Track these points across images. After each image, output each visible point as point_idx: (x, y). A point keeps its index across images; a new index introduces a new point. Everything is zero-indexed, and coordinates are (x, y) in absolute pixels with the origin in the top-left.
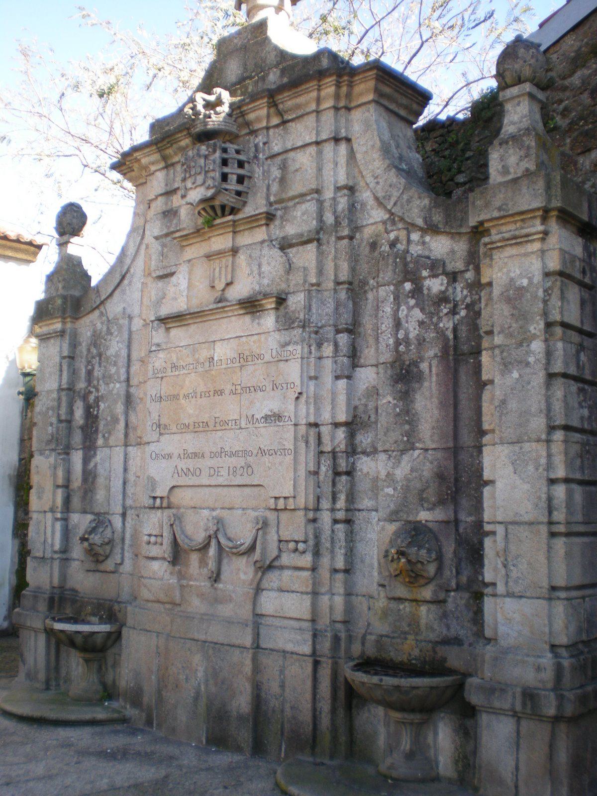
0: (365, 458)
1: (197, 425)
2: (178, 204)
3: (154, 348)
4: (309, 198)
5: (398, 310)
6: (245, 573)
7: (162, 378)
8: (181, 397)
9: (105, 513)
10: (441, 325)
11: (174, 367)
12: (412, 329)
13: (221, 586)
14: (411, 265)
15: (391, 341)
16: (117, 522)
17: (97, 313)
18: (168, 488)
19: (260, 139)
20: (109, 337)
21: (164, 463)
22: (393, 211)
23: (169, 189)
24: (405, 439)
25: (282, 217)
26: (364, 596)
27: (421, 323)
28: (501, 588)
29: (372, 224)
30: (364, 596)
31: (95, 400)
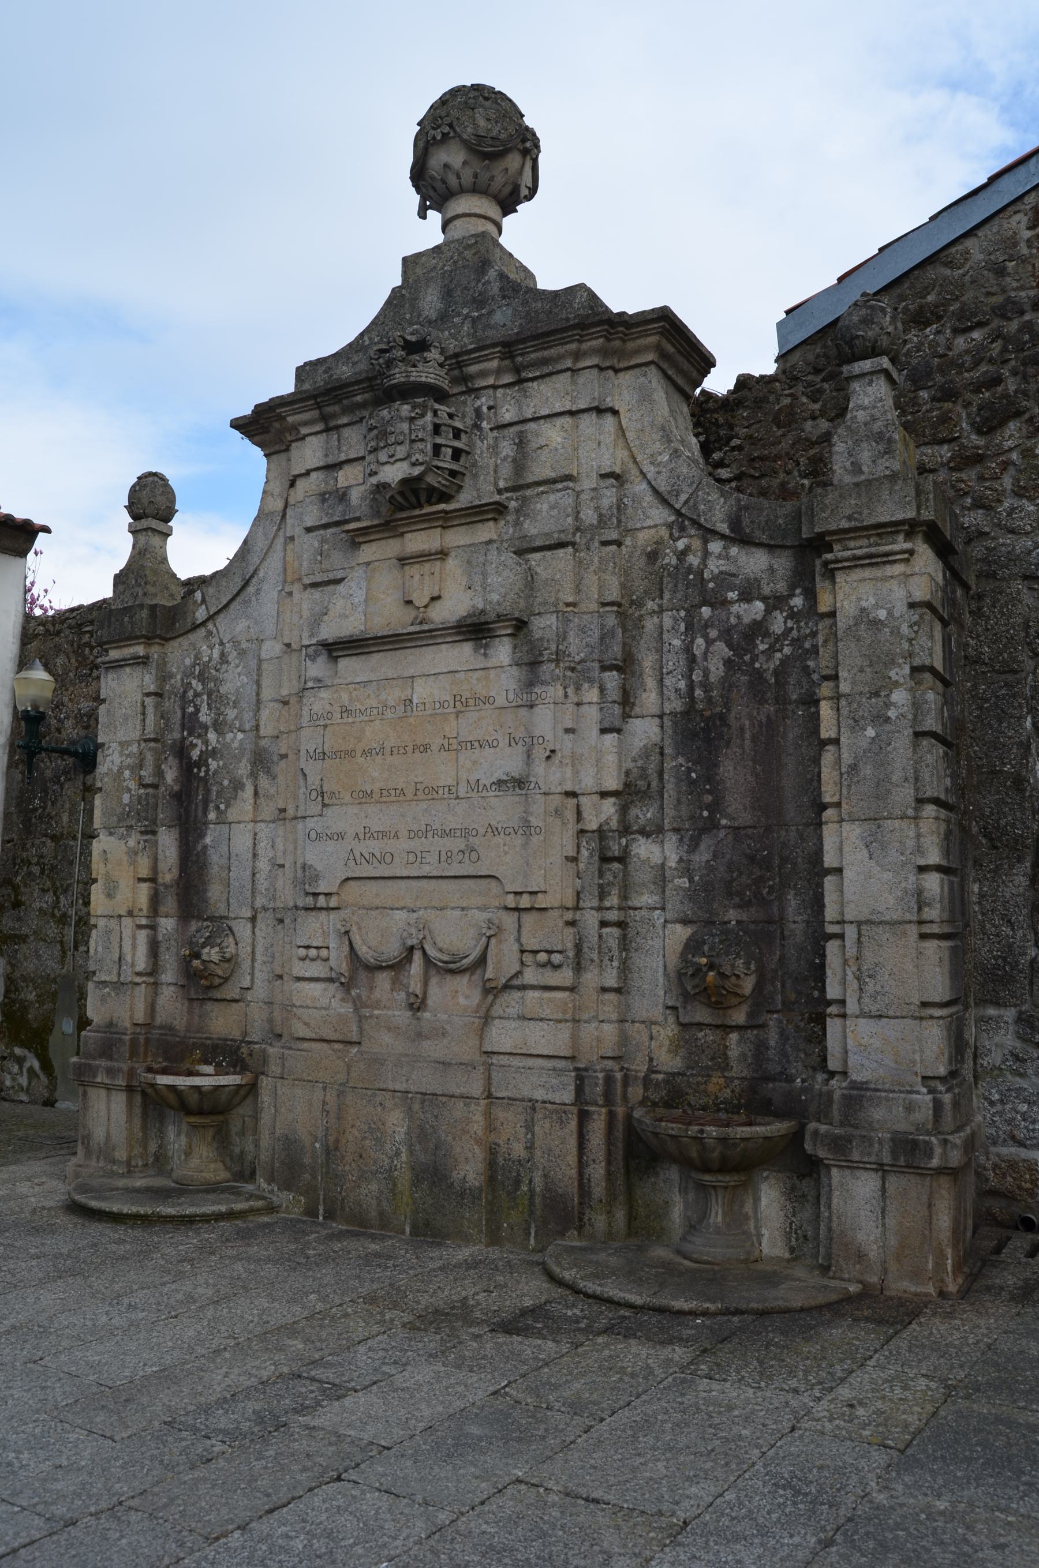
0: (642, 840)
1: (385, 793)
2: (346, 484)
3: (310, 684)
4: (560, 486)
5: (692, 642)
6: (467, 997)
7: (325, 726)
8: (359, 754)
9: (221, 917)
10: (757, 665)
11: (345, 711)
12: (716, 669)
13: (427, 1015)
14: (711, 585)
15: (682, 685)
16: (243, 930)
17: (202, 632)
18: (339, 882)
19: (483, 402)
20: (224, 666)
21: (331, 846)
22: (683, 511)
23: (331, 460)
24: (705, 814)
25: (518, 511)
26: (643, 1022)
27: (728, 663)
28: (852, 1007)
29: (649, 527)
30: (643, 1022)
31: (200, 756)
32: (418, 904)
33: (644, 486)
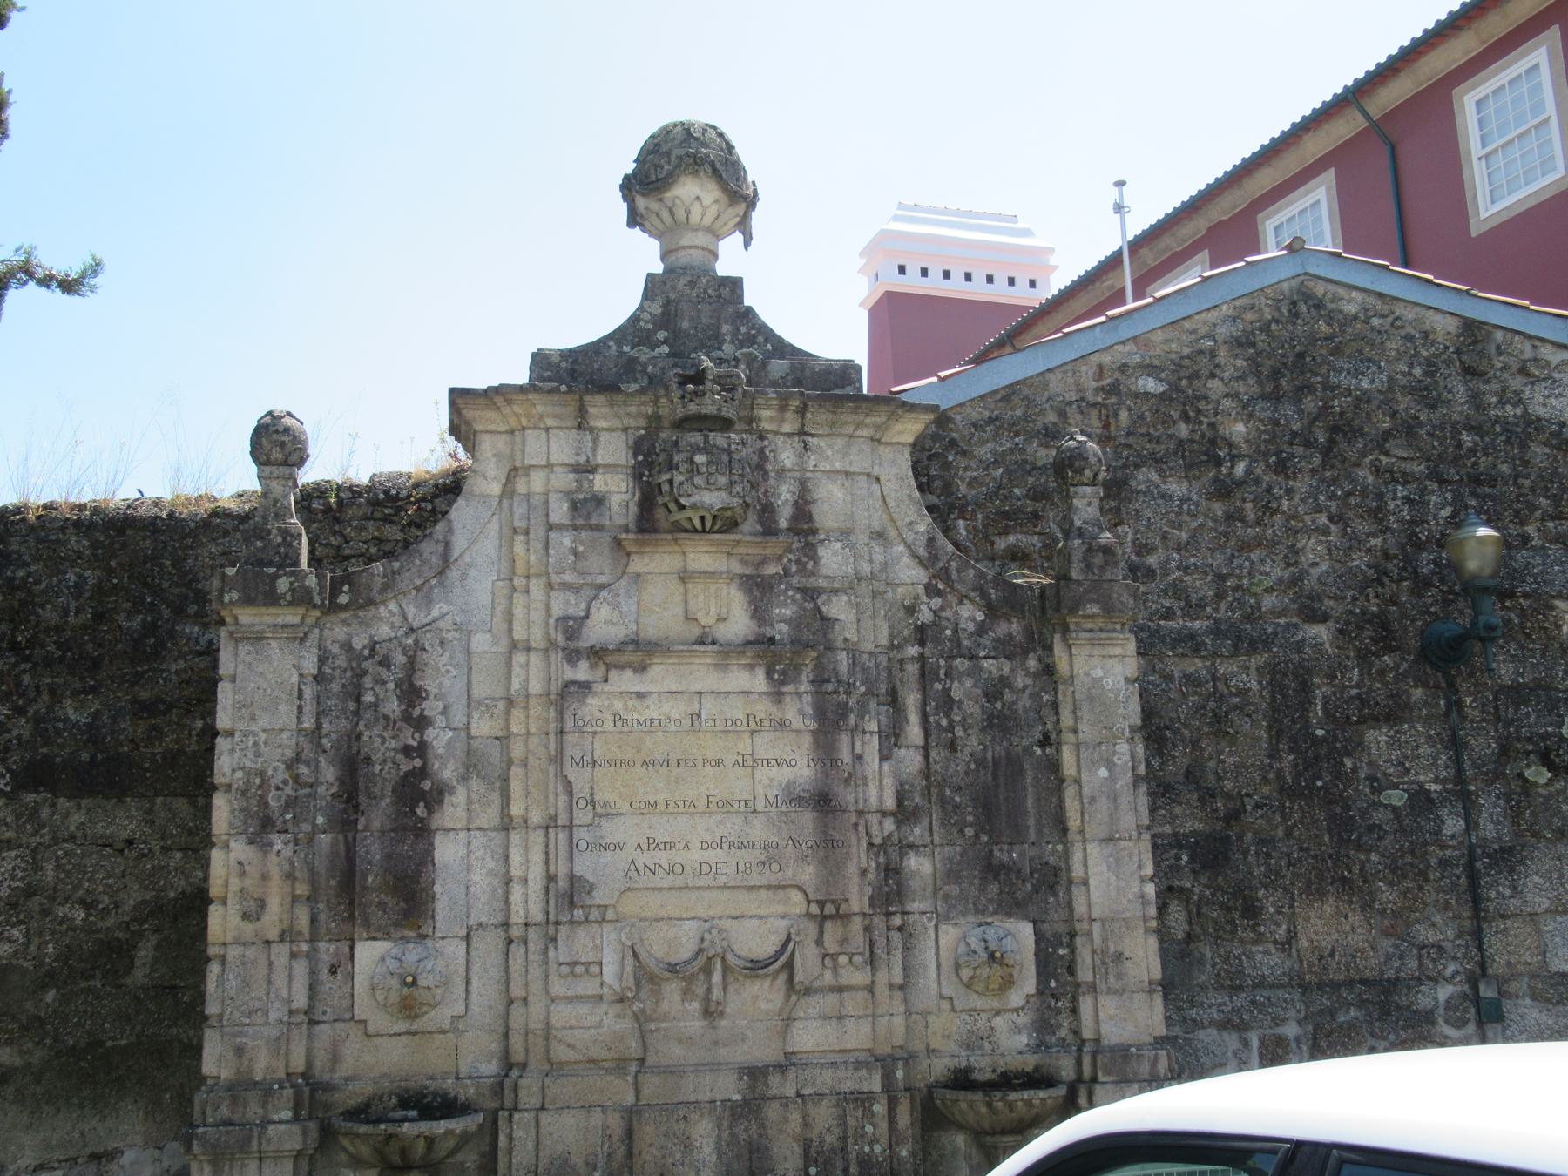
0: (912, 854)
1: (672, 804)
7: (595, 733)
8: (638, 764)
11: (617, 718)
13: (724, 1023)
28: (1101, 986)
32: (711, 913)
33: (901, 548)
